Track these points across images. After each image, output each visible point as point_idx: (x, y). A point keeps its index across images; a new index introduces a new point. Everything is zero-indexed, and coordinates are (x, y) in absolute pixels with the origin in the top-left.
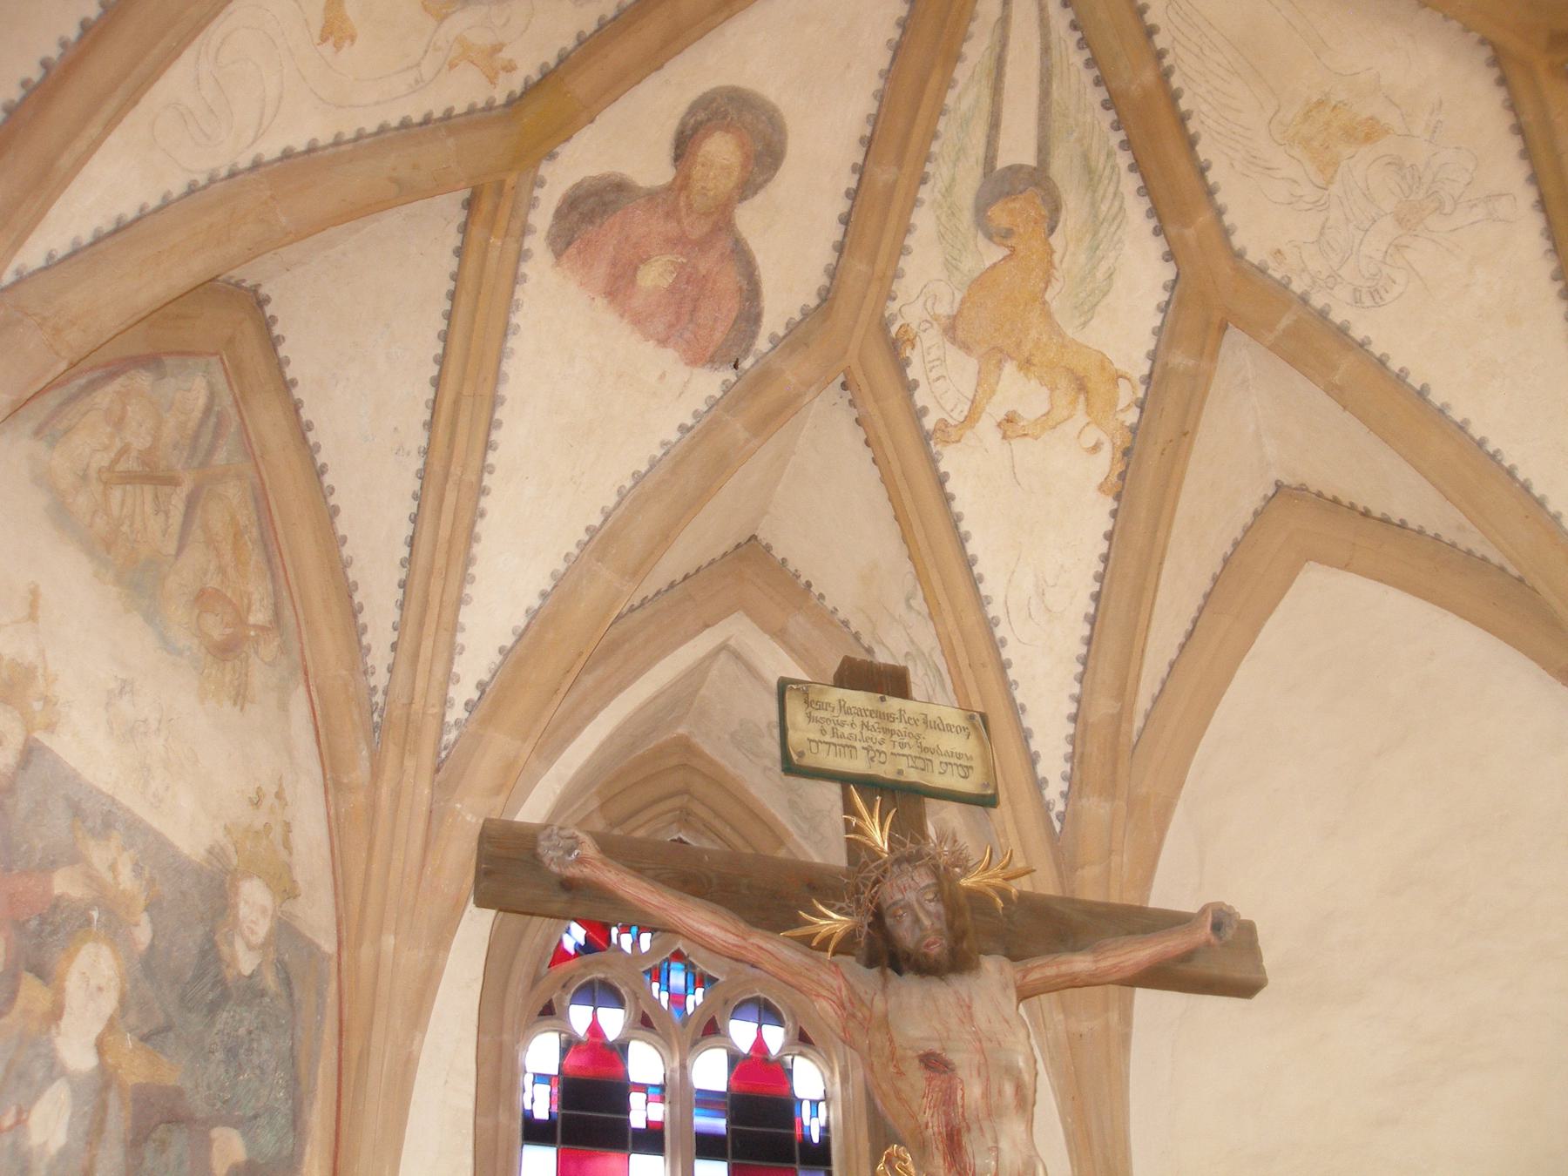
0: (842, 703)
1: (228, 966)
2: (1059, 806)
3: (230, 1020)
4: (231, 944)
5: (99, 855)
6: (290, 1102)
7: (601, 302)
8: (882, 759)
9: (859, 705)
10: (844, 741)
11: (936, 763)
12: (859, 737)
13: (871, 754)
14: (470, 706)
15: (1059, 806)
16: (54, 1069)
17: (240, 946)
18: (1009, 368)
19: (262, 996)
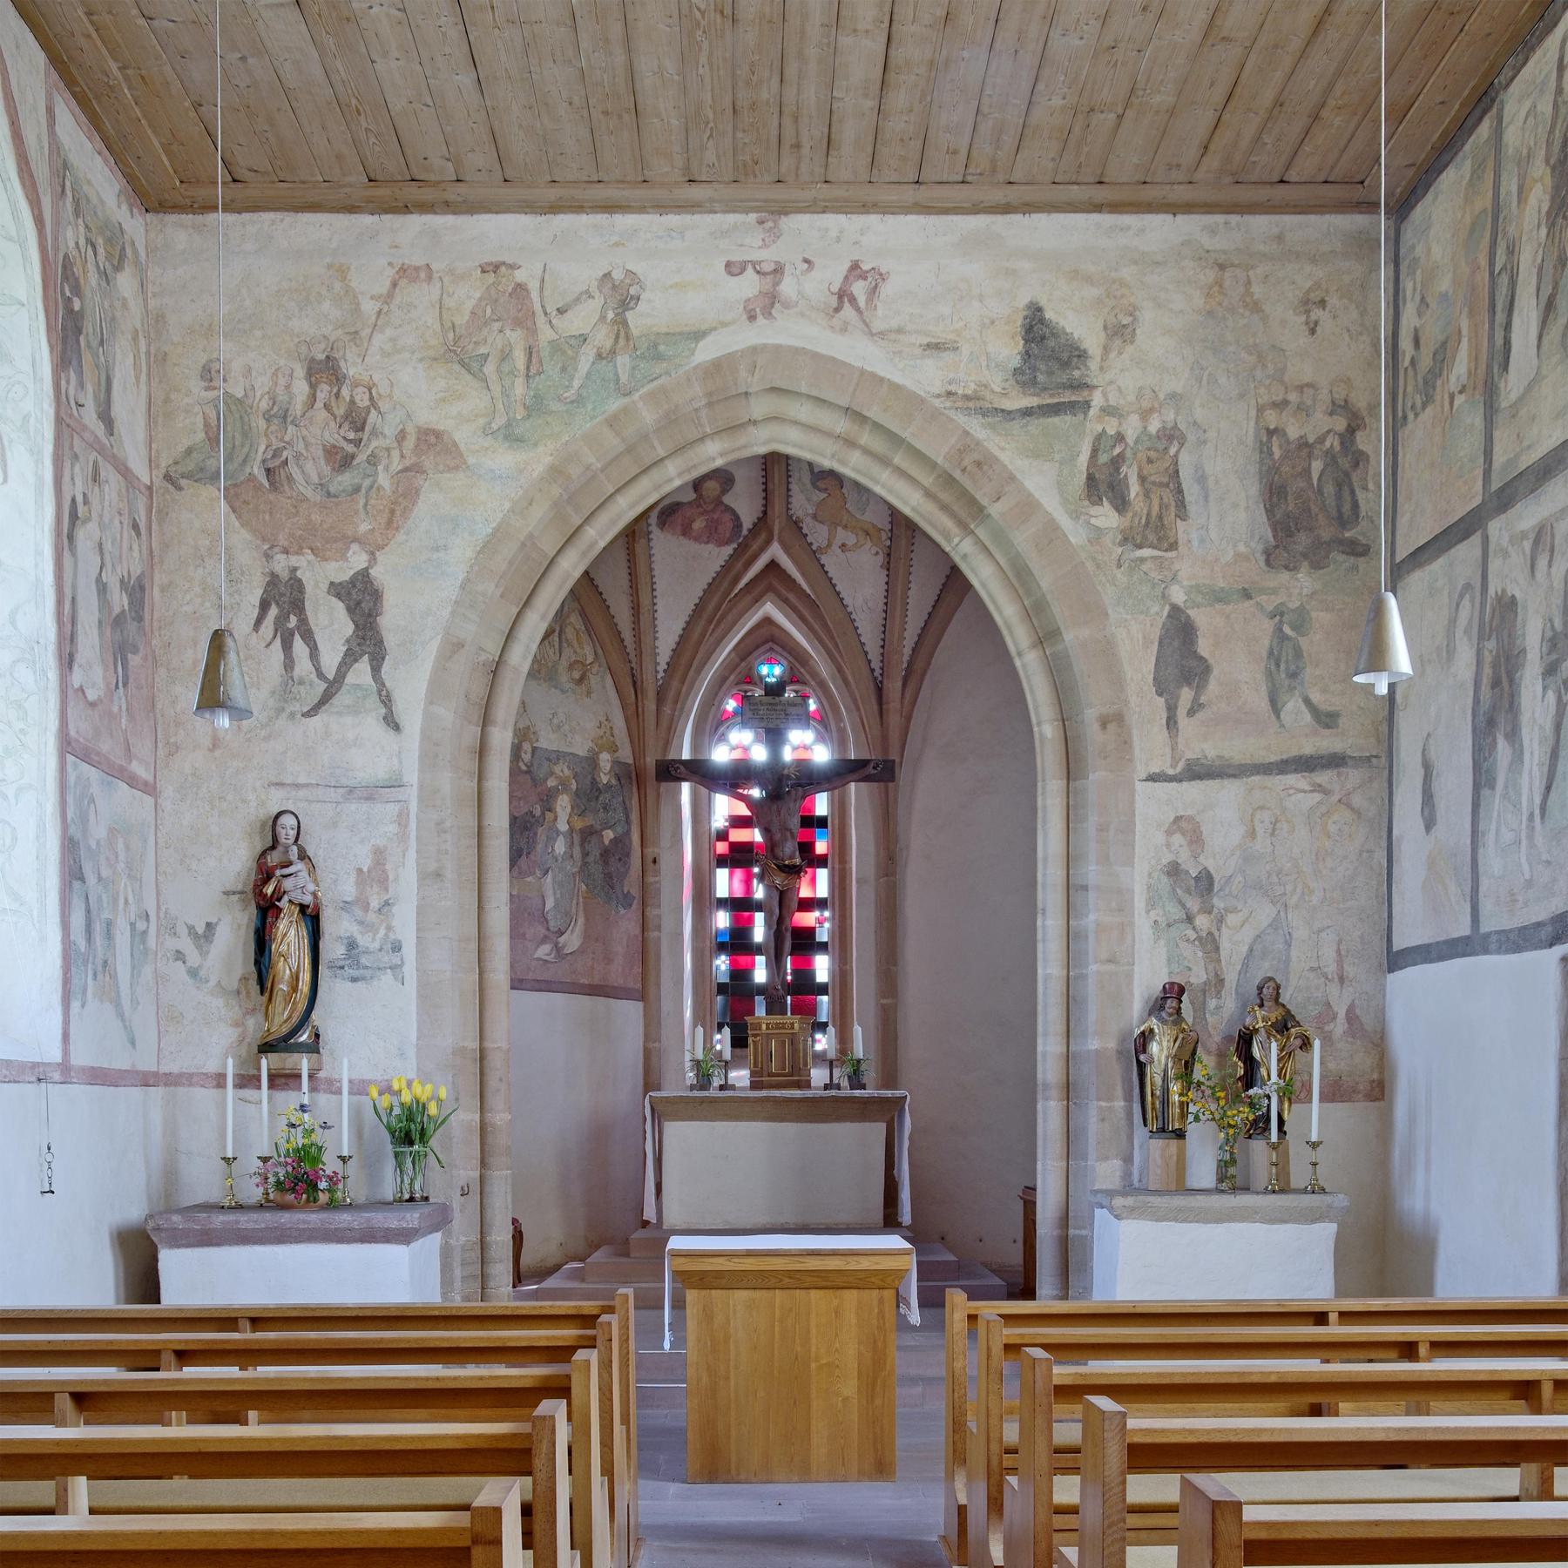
5: (557, 769)
7: (681, 538)
14: (665, 671)
16: (558, 833)
18: (839, 529)
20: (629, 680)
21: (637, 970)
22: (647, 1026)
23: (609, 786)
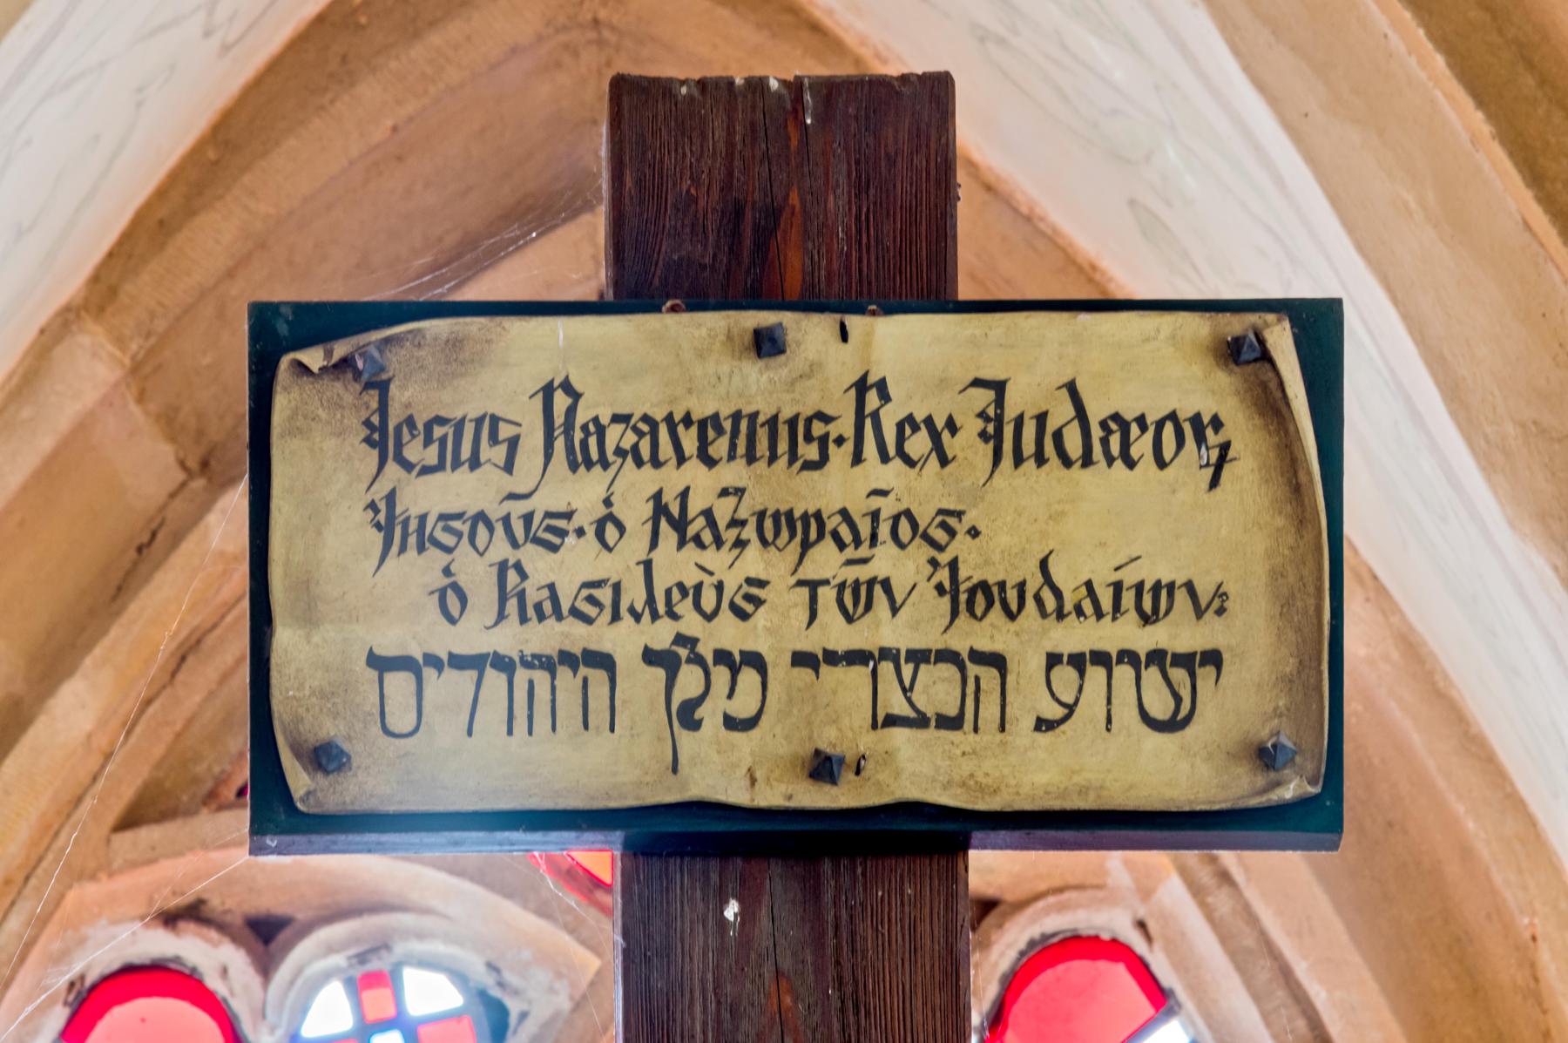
0: (561, 401)
8: (744, 706)
9: (647, 399)
10: (547, 637)
11: (1027, 666)
12: (634, 594)
13: (689, 681)
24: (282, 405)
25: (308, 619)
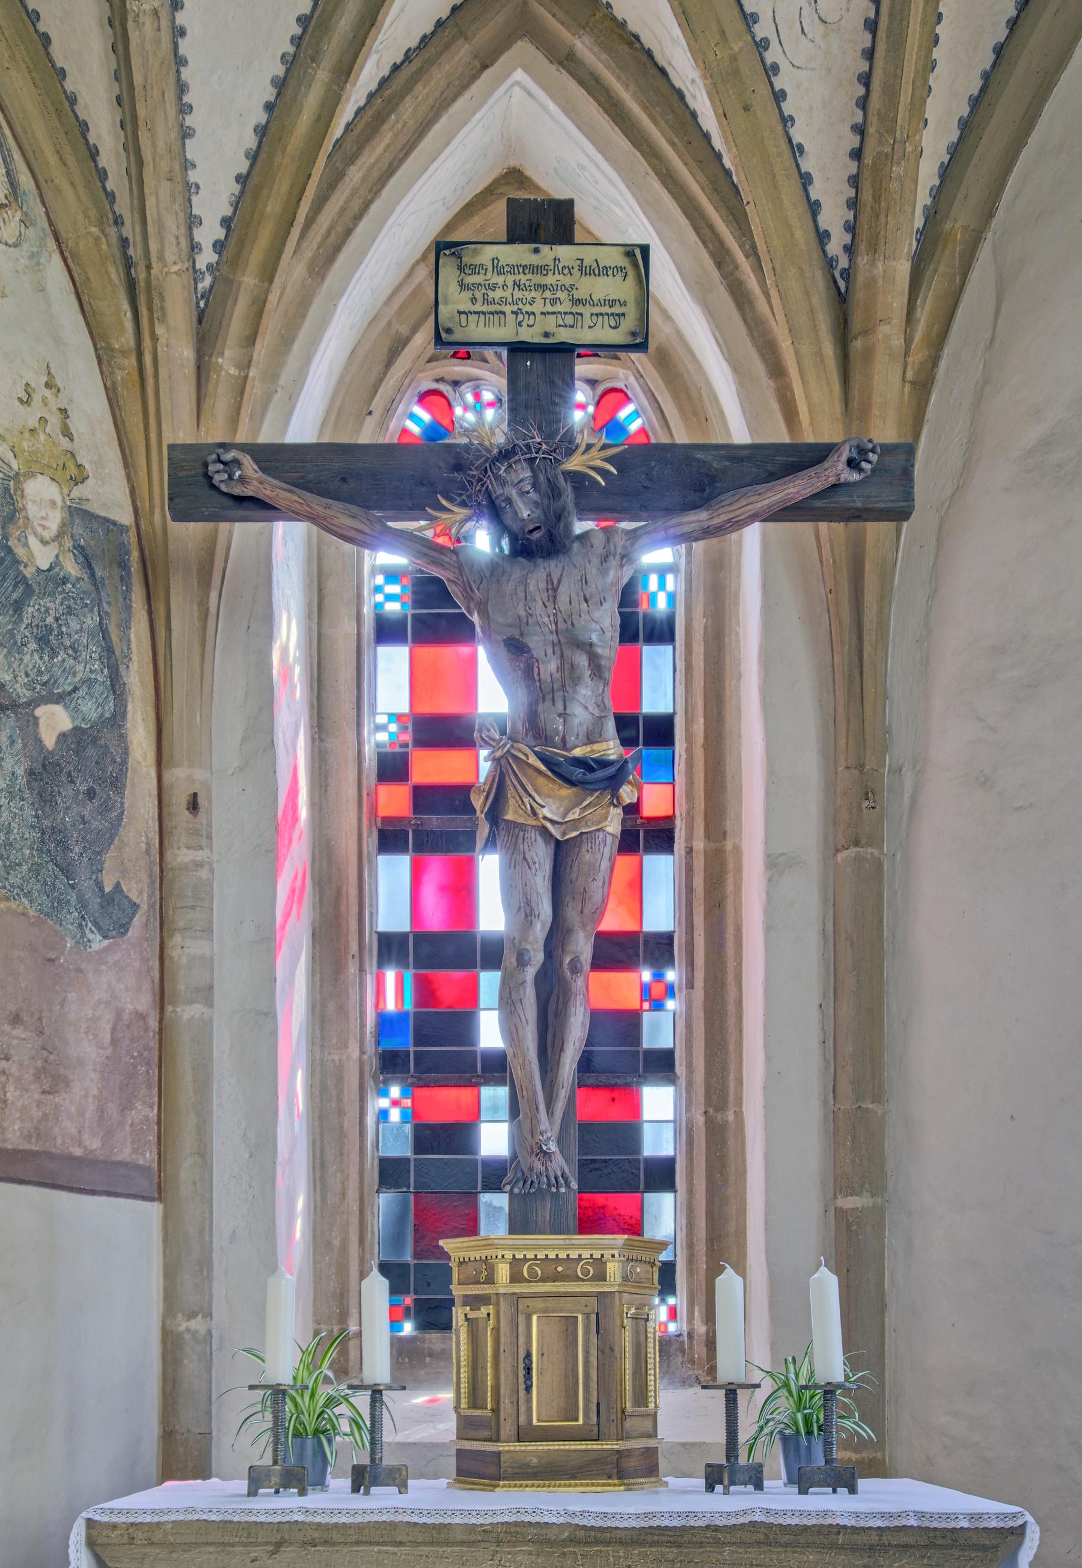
0: (496, 262)
1: (26, 566)
2: (843, 263)
3: (36, 614)
4: (26, 545)
6: (106, 671)
8: (531, 322)
9: (513, 261)
10: (492, 308)
11: (587, 316)
12: (510, 300)
13: (520, 318)
15: (843, 263)
17: (33, 542)
19: (64, 584)
20: (115, 274)
21: (144, 1111)
22: (171, 1272)
23: (54, 579)
24: (441, 261)
25: (446, 303)
